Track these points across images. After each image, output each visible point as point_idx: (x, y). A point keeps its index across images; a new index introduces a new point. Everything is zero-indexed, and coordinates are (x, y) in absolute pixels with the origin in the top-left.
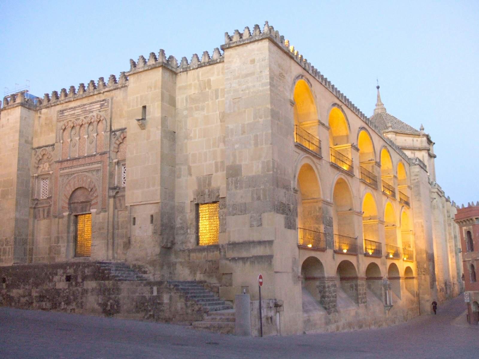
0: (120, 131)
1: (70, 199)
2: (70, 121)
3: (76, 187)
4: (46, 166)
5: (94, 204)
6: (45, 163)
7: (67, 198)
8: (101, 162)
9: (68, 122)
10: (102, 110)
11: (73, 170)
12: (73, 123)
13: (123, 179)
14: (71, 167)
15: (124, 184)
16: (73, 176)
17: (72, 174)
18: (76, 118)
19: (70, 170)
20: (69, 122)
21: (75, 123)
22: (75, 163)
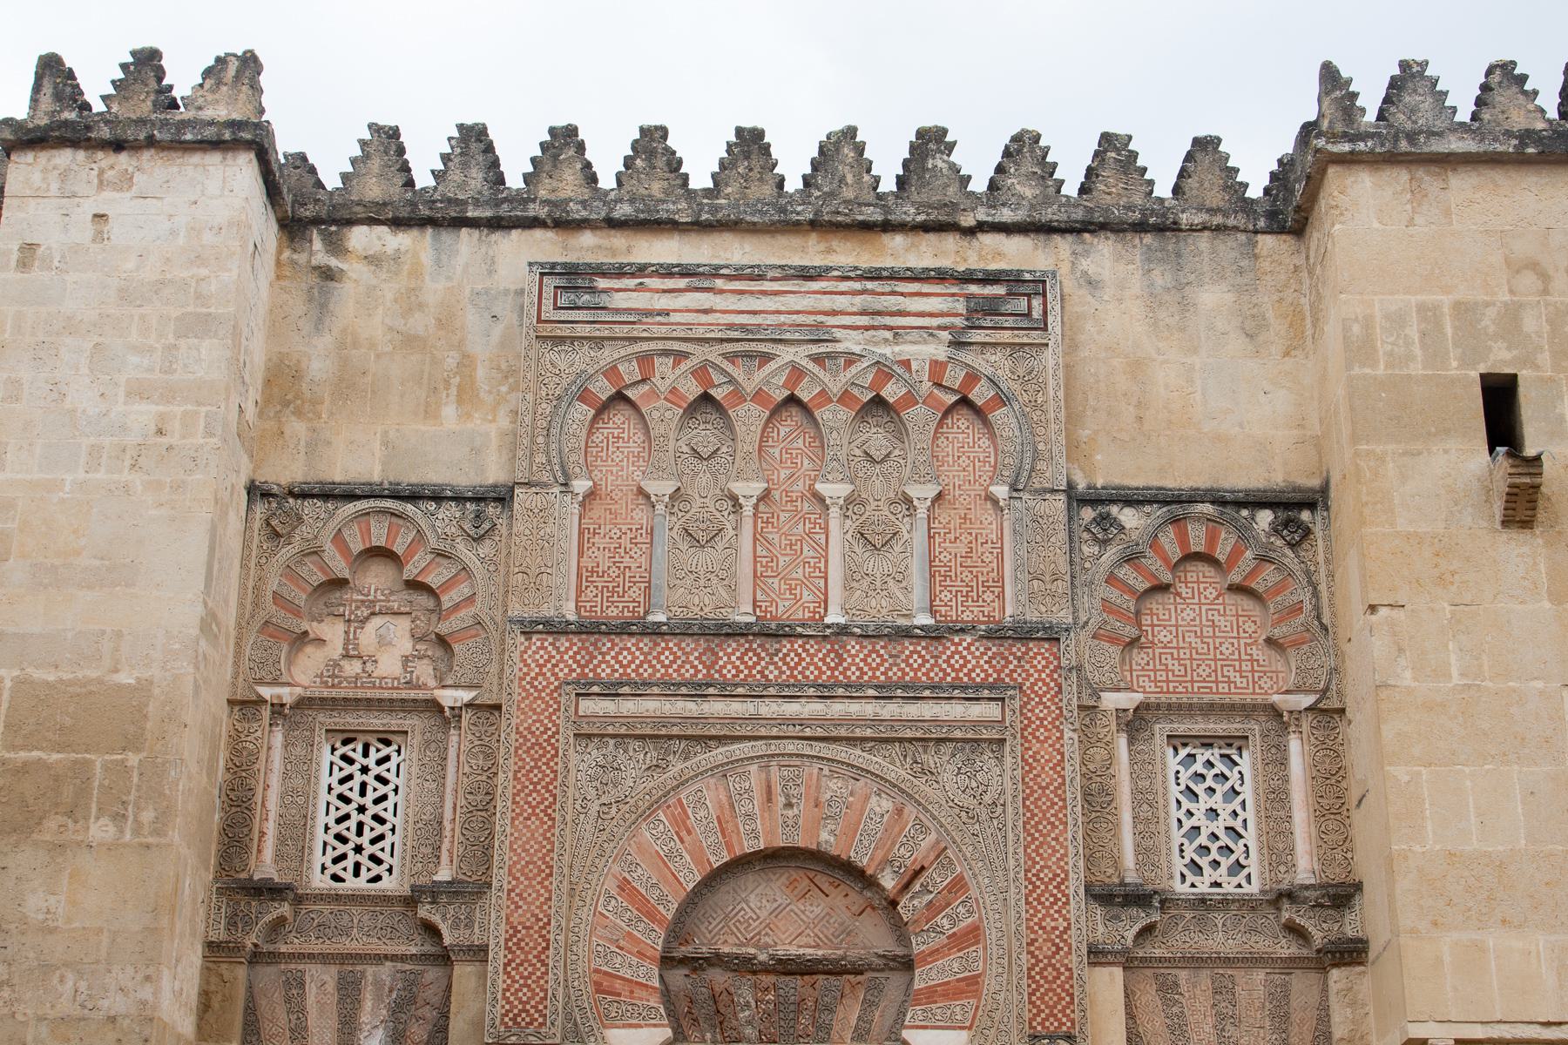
0: (1160, 512)
1: (679, 929)
2: (666, 353)
3: (748, 846)
4: (383, 642)
5: (931, 994)
6: (377, 622)
7: (651, 915)
8: (996, 691)
9: (645, 360)
10: (977, 336)
11: (717, 707)
12: (701, 373)
13: (1177, 836)
14: (698, 690)
15: (1190, 878)
16: (720, 754)
17: (704, 740)
18: (730, 347)
19: (691, 708)
20: (662, 365)
21: (717, 378)
22: (732, 659)
